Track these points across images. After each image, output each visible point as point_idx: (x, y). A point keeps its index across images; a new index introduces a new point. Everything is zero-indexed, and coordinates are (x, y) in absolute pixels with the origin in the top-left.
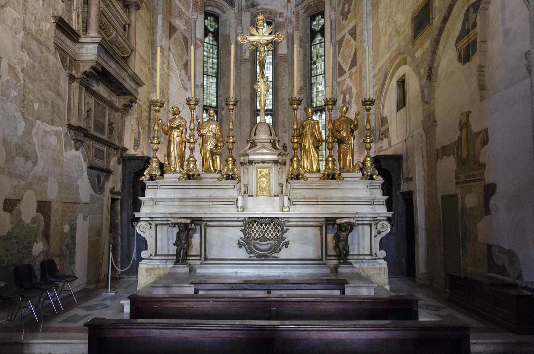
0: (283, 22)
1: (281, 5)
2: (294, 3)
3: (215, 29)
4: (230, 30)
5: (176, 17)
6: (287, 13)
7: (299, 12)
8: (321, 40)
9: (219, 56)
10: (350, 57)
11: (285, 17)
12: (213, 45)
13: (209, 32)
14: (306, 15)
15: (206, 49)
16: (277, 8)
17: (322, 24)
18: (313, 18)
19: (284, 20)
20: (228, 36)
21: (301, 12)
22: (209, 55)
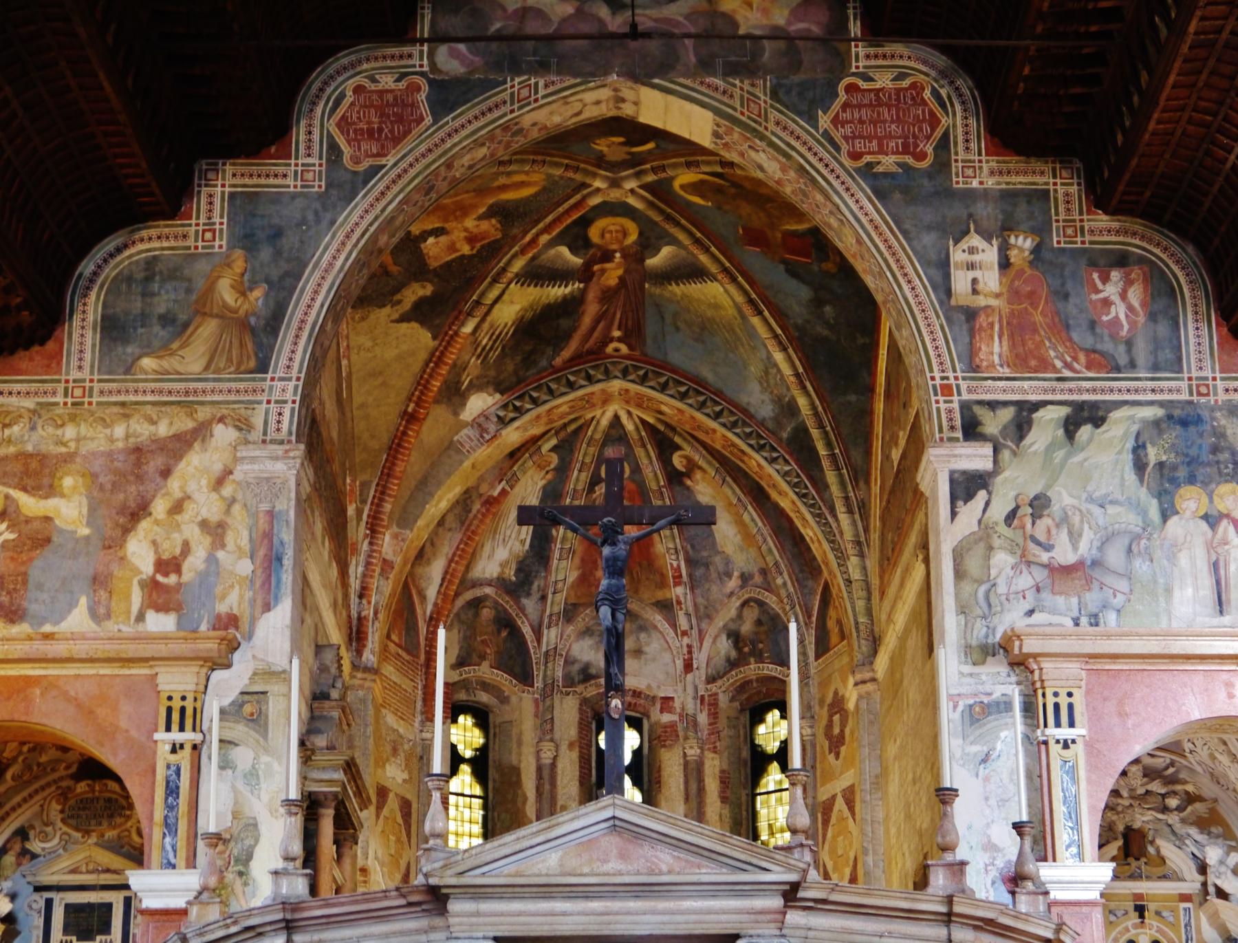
0: (673, 725)
1: (667, 673)
2: (703, 672)
3: (476, 750)
4: (520, 754)
5: (388, 760)
6: (685, 700)
7: (716, 700)
8: (781, 782)
9: (490, 827)
10: (847, 862)
11: (678, 710)
12: (471, 796)
13: (462, 760)
14: (737, 704)
15: (452, 810)
16: (654, 685)
17: (783, 738)
18: (757, 717)
19: (675, 718)
20: (516, 771)
21: (723, 700)
22: (460, 830)
